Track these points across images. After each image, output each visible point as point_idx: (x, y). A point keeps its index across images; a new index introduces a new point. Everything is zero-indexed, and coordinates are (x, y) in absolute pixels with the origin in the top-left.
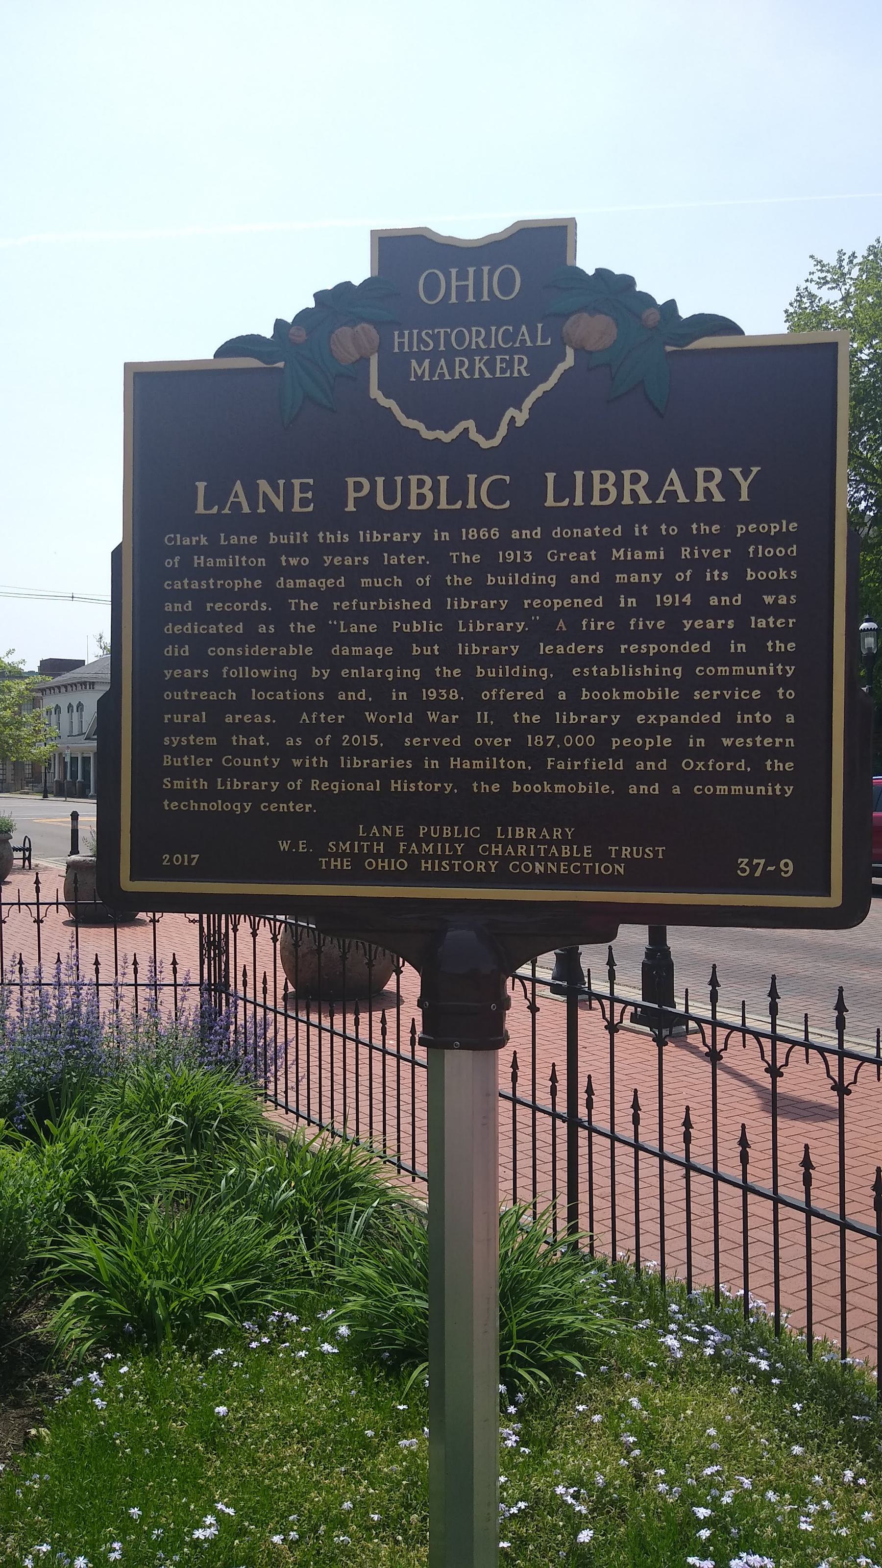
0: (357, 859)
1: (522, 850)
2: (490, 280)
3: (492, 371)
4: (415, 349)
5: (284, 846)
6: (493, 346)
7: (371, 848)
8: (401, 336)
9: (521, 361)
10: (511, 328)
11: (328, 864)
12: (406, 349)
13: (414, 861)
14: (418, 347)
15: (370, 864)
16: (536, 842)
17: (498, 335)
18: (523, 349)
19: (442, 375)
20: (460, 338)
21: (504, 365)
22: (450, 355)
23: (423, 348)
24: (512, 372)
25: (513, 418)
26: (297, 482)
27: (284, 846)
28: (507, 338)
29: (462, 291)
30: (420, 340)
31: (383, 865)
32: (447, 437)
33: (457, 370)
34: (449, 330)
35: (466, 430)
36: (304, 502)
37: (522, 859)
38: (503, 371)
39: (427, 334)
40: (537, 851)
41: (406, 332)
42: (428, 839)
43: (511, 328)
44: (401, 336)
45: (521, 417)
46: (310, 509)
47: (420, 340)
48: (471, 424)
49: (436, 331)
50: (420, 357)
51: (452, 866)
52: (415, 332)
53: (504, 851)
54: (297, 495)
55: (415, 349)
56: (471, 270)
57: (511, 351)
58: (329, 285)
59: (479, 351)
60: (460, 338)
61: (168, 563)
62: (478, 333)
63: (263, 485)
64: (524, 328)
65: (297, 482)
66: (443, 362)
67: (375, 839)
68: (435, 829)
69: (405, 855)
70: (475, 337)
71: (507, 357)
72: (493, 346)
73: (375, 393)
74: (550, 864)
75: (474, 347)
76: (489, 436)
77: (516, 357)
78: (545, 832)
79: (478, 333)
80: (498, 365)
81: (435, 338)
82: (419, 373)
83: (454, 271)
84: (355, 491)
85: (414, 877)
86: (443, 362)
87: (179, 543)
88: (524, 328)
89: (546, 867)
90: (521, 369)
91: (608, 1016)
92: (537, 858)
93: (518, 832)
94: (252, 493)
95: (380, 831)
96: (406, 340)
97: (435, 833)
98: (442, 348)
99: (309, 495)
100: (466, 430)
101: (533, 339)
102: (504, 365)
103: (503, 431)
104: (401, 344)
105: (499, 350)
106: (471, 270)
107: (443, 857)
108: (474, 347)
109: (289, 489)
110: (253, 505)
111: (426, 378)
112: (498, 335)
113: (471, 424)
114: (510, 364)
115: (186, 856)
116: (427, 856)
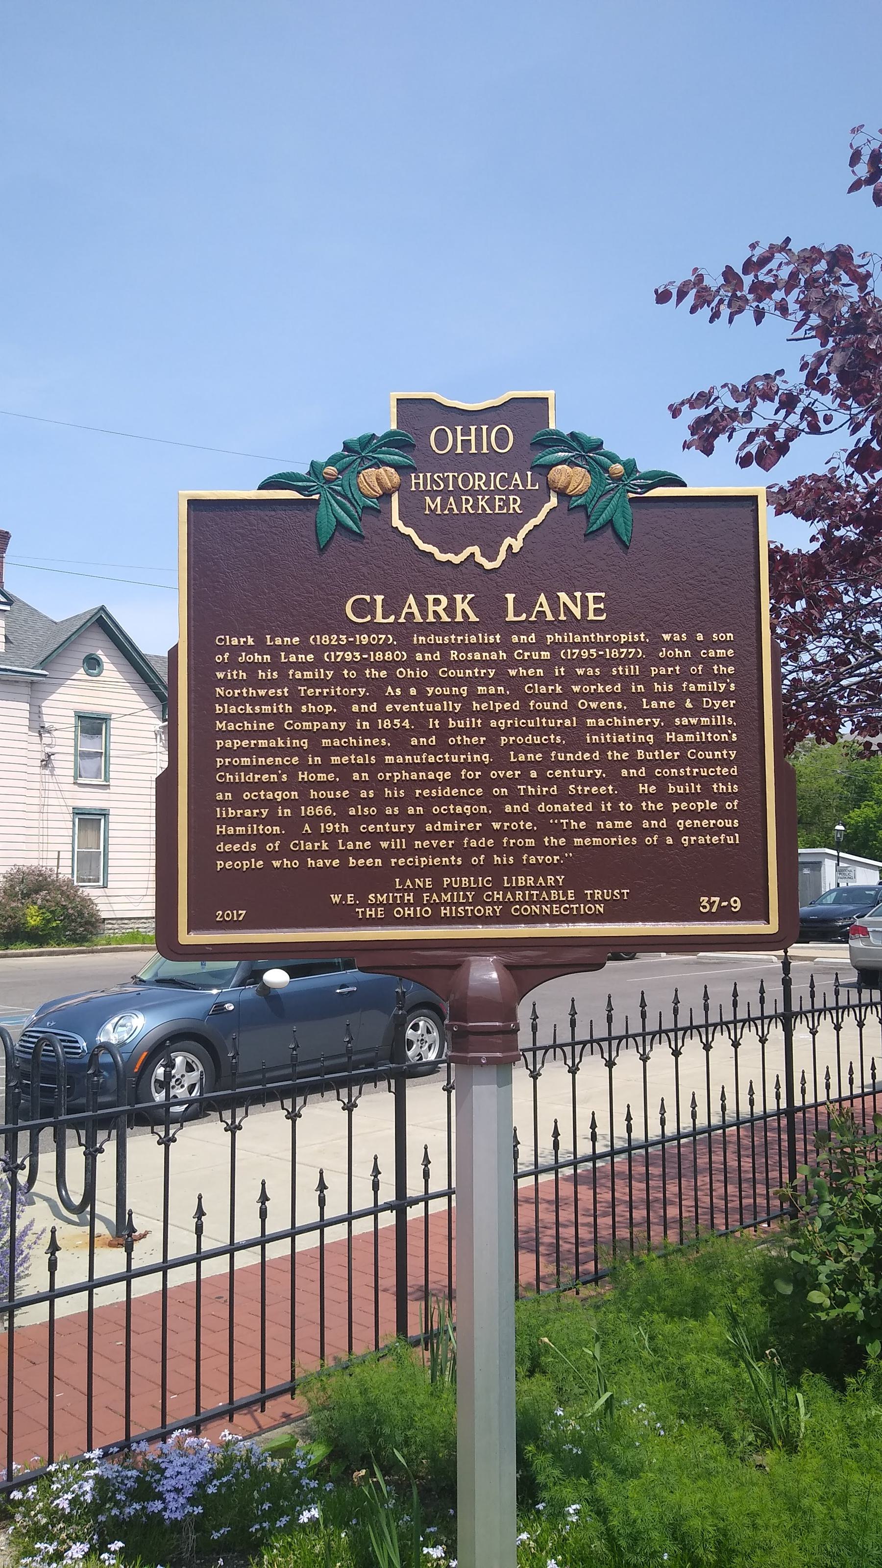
0: (388, 908)
1: (519, 895)
2: (490, 437)
3: (492, 508)
4: (429, 488)
5: (336, 899)
6: (492, 488)
7: (402, 898)
8: (417, 478)
9: (515, 501)
10: (506, 474)
11: (364, 913)
12: (422, 489)
13: (435, 906)
14: (431, 487)
15: (399, 912)
16: (531, 888)
17: (496, 480)
18: (516, 492)
19: (451, 509)
20: (466, 481)
21: (501, 504)
22: (458, 493)
23: (435, 488)
24: (508, 510)
25: (510, 547)
26: (590, 596)
27: (336, 899)
28: (504, 481)
29: (466, 443)
30: (433, 481)
31: (409, 912)
32: (457, 559)
33: (464, 506)
34: (456, 474)
35: (473, 555)
36: (597, 611)
37: (520, 903)
38: (501, 508)
39: (438, 477)
40: (531, 895)
41: (421, 475)
42: (450, 888)
43: (506, 474)
44: (417, 478)
45: (517, 545)
46: (603, 618)
47: (433, 481)
48: (476, 549)
49: (446, 474)
50: (433, 495)
51: (466, 911)
52: (429, 475)
53: (504, 898)
54: (592, 606)
55: (429, 488)
56: (473, 428)
57: (508, 493)
58: (354, 435)
59: (481, 492)
60: (466, 481)
61: (219, 659)
62: (480, 478)
63: (563, 597)
64: (517, 475)
65: (590, 596)
66: (451, 499)
67: (471, 889)
68: (456, 881)
69: (429, 904)
70: (477, 481)
71: (504, 497)
72: (492, 488)
73: (396, 522)
74: (544, 906)
75: (477, 488)
76: (492, 559)
77: (511, 497)
78: (541, 880)
79: (480, 478)
80: (497, 504)
81: (445, 480)
82: (433, 507)
83: (459, 428)
84: (434, 599)
85: (436, 920)
86: (451, 499)
87: (228, 644)
88: (517, 475)
89: (541, 908)
90: (515, 508)
91: (835, 1021)
92: (531, 903)
93: (520, 881)
94: (554, 602)
95: (413, 883)
96: (421, 481)
97: (456, 884)
98: (451, 488)
99: (602, 606)
100: (473, 555)
101: (525, 484)
102: (501, 504)
103: (502, 555)
104: (417, 484)
105: (497, 491)
106: (473, 428)
107: (459, 904)
108: (477, 488)
109: (584, 599)
110: (555, 612)
111: (439, 512)
112: (496, 480)
113: (476, 549)
114: (506, 503)
115: (235, 912)
116: (446, 904)
